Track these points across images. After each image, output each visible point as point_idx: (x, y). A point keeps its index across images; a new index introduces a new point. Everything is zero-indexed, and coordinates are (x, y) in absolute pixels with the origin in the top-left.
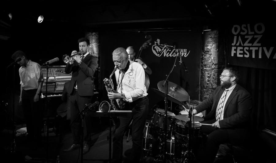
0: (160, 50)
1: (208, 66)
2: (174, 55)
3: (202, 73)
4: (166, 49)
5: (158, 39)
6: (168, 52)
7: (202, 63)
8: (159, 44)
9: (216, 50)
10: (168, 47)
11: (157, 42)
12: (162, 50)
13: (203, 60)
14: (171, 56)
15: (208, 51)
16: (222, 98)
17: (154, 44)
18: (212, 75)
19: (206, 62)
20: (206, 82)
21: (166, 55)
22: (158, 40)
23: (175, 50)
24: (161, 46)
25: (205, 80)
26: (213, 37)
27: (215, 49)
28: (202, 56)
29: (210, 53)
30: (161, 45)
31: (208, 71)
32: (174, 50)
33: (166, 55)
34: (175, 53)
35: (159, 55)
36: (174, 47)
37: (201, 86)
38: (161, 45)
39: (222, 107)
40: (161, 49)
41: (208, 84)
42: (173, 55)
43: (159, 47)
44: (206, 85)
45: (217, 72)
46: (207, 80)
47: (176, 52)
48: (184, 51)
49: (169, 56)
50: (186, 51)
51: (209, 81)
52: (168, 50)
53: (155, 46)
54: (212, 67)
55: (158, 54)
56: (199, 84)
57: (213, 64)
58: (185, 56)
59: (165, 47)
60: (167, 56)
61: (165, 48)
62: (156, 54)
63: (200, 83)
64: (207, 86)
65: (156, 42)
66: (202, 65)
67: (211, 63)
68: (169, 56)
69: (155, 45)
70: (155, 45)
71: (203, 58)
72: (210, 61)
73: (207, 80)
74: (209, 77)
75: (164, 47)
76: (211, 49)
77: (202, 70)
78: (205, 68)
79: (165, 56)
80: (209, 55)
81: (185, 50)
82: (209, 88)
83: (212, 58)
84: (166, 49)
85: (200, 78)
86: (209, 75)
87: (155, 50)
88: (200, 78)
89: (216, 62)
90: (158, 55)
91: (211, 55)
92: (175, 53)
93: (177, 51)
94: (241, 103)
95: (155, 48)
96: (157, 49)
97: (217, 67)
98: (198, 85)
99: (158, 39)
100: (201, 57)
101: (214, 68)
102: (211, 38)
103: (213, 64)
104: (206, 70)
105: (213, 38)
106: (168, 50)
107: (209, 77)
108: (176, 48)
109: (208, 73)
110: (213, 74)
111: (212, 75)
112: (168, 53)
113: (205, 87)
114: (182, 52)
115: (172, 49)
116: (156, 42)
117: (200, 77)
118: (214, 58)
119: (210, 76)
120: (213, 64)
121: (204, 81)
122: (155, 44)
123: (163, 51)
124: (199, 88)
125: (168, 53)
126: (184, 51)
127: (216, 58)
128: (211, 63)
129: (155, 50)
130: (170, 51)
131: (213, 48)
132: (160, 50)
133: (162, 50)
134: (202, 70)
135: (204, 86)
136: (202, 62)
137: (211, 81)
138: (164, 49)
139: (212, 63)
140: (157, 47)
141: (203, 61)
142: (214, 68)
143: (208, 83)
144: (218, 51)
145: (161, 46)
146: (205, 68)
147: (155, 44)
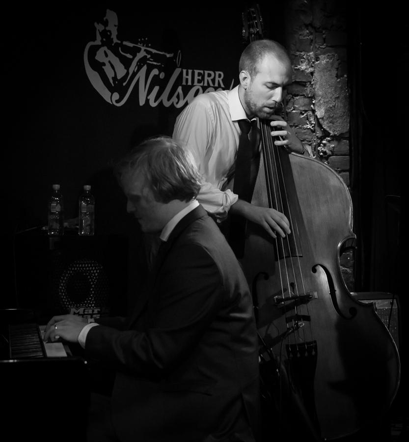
0: (121, 72)
2: (178, 97)
4: (144, 68)
5: (108, 11)
6: (156, 81)
8: (115, 40)
9: (337, 76)
10: (155, 57)
11: (106, 24)
12: (131, 72)
14: (167, 104)
15: (303, 84)
17: (94, 39)
21: (147, 101)
22: (112, 18)
23: (181, 73)
24: (127, 49)
26: (317, 24)
27: (334, 72)
29: (308, 90)
30: (125, 43)
32: (177, 71)
33: (147, 101)
34: (180, 90)
35: (116, 96)
36: (175, 57)
38: (125, 43)
40: (127, 63)
42: (174, 99)
43: (117, 54)
45: (348, 168)
47: (184, 83)
48: (213, 81)
49: (161, 103)
50: (220, 80)
52: (155, 72)
53: (97, 48)
54: (319, 148)
55: (112, 90)
57: (326, 134)
59: (141, 54)
60: (153, 104)
61: (143, 61)
62: (105, 94)
65: (100, 27)
68: (161, 103)
69: (98, 42)
70: (98, 42)
72: (309, 126)
75: (140, 55)
76: (312, 73)
79: (142, 102)
80: (307, 100)
81: (217, 73)
83: (320, 113)
84: (145, 68)
87: (98, 67)
89: (340, 127)
90: (110, 97)
91: (313, 97)
92: (180, 90)
93: (187, 75)
95: (100, 56)
96: (108, 65)
97: (345, 146)
99: (108, 11)
101: (333, 155)
102: (307, 26)
103: (322, 139)
105: (317, 30)
106: (155, 72)
108: (182, 67)
112: (156, 89)
114: (209, 86)
115: (168, 67)
116: (100, 27)
118: (327, 111)
122: (99, 38)
123: (134, 74)
125: (156, 89)
126: (214, 82)
127: (340, 107)
128: (314, 131)
129: (98, 67)
130: (162, 76)
131: (325, 69)
132: (121, 72)
133: (131, 72)
138: (140, 67)
139: (319, 134)
140: (109, 52)
144: (350, 84)
145: (127, 49)
147: (99, 38)
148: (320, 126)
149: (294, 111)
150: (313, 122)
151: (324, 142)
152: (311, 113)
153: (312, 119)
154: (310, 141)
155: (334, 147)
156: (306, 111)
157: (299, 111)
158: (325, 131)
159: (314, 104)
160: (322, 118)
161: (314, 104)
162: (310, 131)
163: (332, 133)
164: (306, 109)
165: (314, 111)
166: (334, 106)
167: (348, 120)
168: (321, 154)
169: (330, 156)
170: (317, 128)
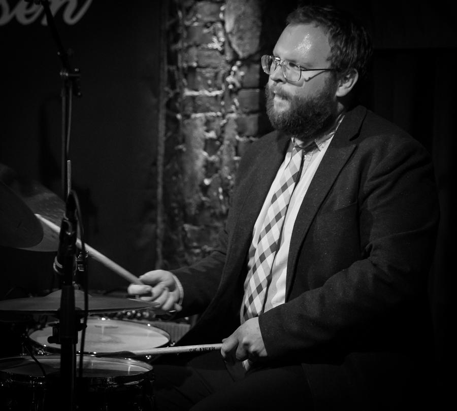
1: (208, 73)
3: (174, 125)
7: (172, 60)
13: (176, 41)
16: (275, 198)
18: (231, 133)
19: (194, 51)
20: (193, 178)
25: (189, 172)
28: (173, 14)
31: (207, 110)
37: (169, 212)
39: (276, 248)
41: (205, 189)
44: (194, 199)
45: (257, 107)
46: (199, 164)
51: (211, 168)
54: (230, 79)
56: (155, 196)
57: (236, 57)
58: (68, 20)
63: (160, 191)
64: (201, 206)
66: (171, 75)
67: (223, 53)
71: (175, 26)
73: (199, 164)
74: (211, 146)
77: (170, 105)
78: (188, 93)
82: (214, 215)
83: (229, 26)
85: (161, 159)
86: (212, 135)
88: (161, 159)
94: (379, 197)
98: (150, 206)
100: (168, 24)
101: (243, 87)
103: (232, 63)
104: (196, 104)
107: (211, 146)
109: (208, 123)
110: (236, 120)
111: (231, 133)
113: (193, 211)
117: (161, 150)
118: (237, 21)
119: (220, 138)
120: (236, 57)
121: (182, 171)
124: (154, 221)
134: (170, 105)
135: (183, 207)
136: (169, 51)
137: (225, 170)
139: (229, 56)
141: (179, 45)
142: (243, 87)
143: (207, 182)
146: (188, 93)
148: (230, 44)
149: (196, 24)
150: (222, 39)
151: (235, 68)
152: (219, 25)
153: (221, 34)
154: (215, 68)
155: (243, 77)
156: (212, 23)
157: (202, 24)
158: (235, 53)
159: (224, 12)
160: (231, 33)
161: (224, 12)
162: (218, 54)
163: (241, 54)
164: (213, 19)
165: (223, 23)
166: (244, 13)
167: (258, 34)
168: (231, 87)
169: (239, 89)
170: (227, 48)
